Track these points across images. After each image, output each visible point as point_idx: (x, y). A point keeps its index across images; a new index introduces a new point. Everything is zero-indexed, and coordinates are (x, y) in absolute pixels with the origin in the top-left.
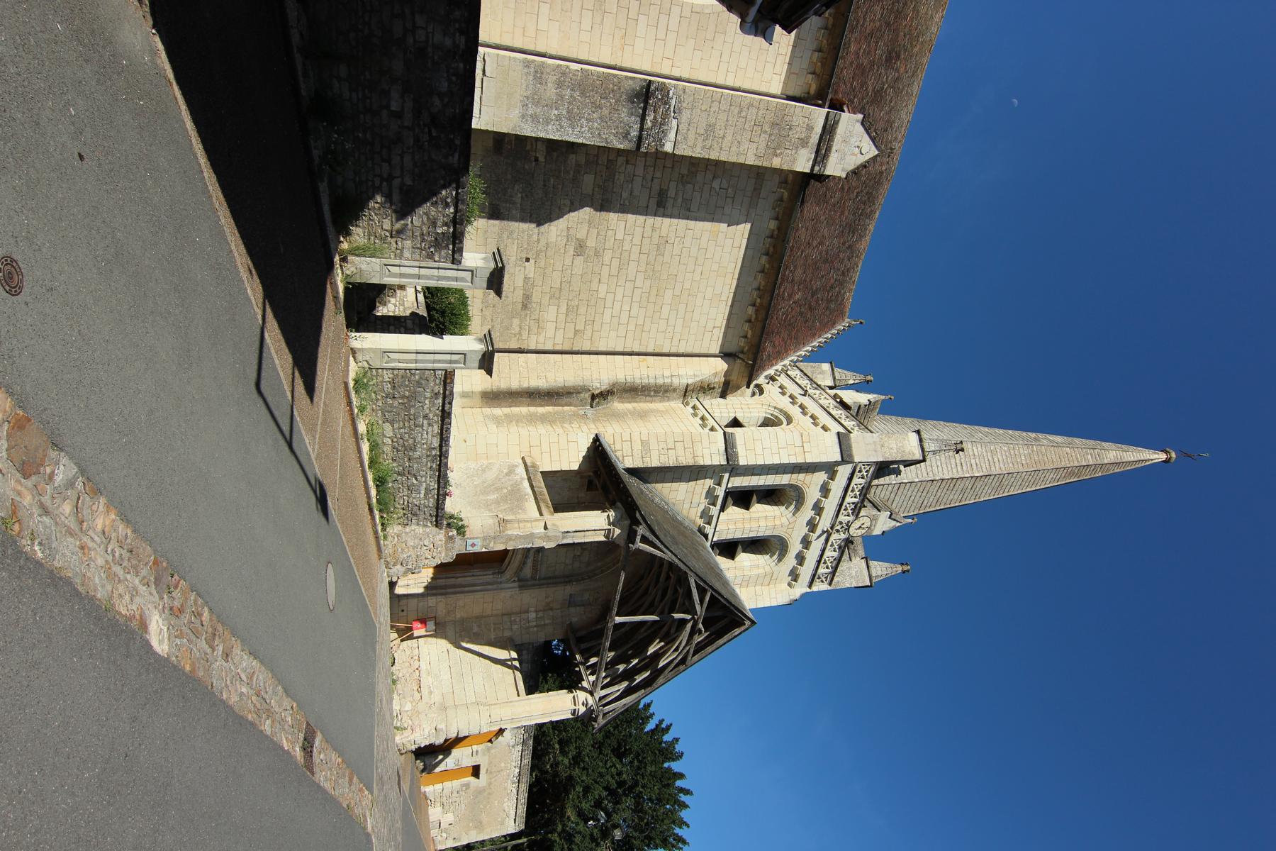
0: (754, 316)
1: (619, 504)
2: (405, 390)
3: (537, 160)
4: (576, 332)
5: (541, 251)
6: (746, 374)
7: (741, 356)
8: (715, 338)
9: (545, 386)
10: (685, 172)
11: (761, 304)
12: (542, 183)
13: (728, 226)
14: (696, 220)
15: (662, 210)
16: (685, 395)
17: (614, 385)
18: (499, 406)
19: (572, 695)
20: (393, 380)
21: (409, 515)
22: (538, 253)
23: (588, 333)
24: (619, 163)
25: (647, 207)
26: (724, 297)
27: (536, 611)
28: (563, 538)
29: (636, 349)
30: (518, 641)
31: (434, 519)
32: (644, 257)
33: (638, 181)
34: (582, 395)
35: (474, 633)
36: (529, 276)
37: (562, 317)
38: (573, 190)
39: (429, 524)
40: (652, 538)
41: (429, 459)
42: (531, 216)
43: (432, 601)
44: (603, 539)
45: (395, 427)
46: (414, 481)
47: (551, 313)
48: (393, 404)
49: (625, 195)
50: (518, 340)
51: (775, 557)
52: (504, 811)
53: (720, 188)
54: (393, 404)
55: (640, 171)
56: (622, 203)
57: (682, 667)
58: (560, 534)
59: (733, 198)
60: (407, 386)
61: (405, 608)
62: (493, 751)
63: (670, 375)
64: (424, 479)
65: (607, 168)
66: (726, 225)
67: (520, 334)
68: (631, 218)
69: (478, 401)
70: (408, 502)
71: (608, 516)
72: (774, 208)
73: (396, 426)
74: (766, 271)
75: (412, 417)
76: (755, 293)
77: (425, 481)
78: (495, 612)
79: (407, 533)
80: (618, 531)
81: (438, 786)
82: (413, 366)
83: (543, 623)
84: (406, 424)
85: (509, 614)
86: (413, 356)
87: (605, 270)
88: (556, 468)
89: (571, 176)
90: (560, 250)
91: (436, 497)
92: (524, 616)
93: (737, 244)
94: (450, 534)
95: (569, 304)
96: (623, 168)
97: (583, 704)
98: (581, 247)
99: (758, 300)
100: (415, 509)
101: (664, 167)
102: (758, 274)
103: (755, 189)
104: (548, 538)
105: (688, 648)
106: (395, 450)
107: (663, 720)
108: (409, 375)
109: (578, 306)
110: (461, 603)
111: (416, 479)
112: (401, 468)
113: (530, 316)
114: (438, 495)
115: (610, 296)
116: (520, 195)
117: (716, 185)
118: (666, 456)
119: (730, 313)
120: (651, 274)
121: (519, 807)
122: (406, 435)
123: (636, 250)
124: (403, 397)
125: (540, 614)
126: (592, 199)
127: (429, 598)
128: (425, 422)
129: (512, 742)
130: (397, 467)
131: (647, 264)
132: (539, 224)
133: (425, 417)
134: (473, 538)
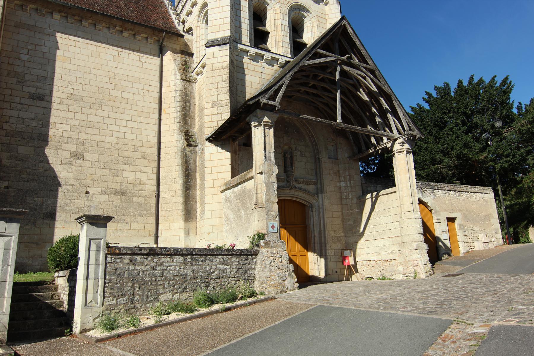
0: (130, 32)
1: (247, 119)
2: (126, 286)
3: (7, 187)
4: (143, 158)
5: (80, 183)
6: (175, 38)
7: (161, 41)
8: (148, 60)
9: (181, 179)
10: (15, 80)
11: (121, 26)
12: (26, 183)
13: (58, 49)
14: (53, 73)
15: (46, 98)
16: (190, 81)
17: (181, 131)
18: (195, 210)
19: (396, 154)
20: (115, 296)
21: (246, 276)
22: (81, 185)
23: (144, 149)
24: (9, 128)
25: (44, 108)
26: (116, 53)
27: (340, 182)
28: (270, 160)
29: (156, 116)
30: (360, 193)
31: (250, 257)
32: (84, 110)
33: (22, 114)
34: (188, 153)
35: (354, 223)
36: (100, 192)
37: (132, 168)
38: (31, 161)
39: (255, 260)
40: (271, 92)
41: (194, 263)
42: (52, 191)
43: (330, 252)
44: (272, 130)
45: (163, 292)
46: (215, 273)
47: (129, 176)
48: (139, 295)
49: (34, 124)
50: (149, 198)
51: (305, 14)
52: (479, 201)
53: (28, 54)
54: (139, 295)
55: (14, 113)
56: (41, 126)
57: (377, 73)
58: (266, 162)
59: (35, 45)
60: (122, 285)
61: (335, 271)
62: (438, 209)
63: (174, 92)
64: (213, 267)
65: (13, 137)
66: (58, 51)
67: (145, 197)
68: (53, 119)
69: (191, 225)
70: (234, 277)
71: (255, 126)
72: (44, 15)
73: (161, 291)
74: (94, 22)
75: (153, 279)
76: (112, 30)
77: (216, 265)
78: (340, 210)
79: (260, 278)
80: (266, 119)
81: (460, 244)
82: (101, 282)
84: (160, 283)
85: (341, 200)
86: (91, 282)
87: (94, 138)
88: (229, 168)
89: (19, 162)
90: (79, 170)
91: (230, 257)
92: (343, 189)
93: (73, 43)
94: (263, 244)
95: (121, 163)
96: (12, 125)
97: (403, 146)
98: (77, 155)
99: (118, 28)
100: (241, 272)
101: (11, 95)
102: (97, 28)
103: (28, 29)
104: (269, 173)
105: (362, 68)
106: (185, 290)
107: (423, 98)
108: (110, 284)
109: (124, 157)
110: (332, 233)
111: (213, 272)
112: (203, 285)
113: (131, 190)
114: (228, 255)
115: (116, 134)
116: (36, 199)
117: (25, 58)
118: (222, 89)
119: (128, 49)
120: (98, 105)
121: (476, 191)
122: (171, 282)
123: (78, 116)
124: (133, 287)
125: (342, 179)
126: (38, 147)
127: (328, 254)
128: (158, 268)
129: (432, 196)
130: (201, 288)
131: (90, 108)
132: (59, 185)
133: (154, 268)
134: (267, 227)
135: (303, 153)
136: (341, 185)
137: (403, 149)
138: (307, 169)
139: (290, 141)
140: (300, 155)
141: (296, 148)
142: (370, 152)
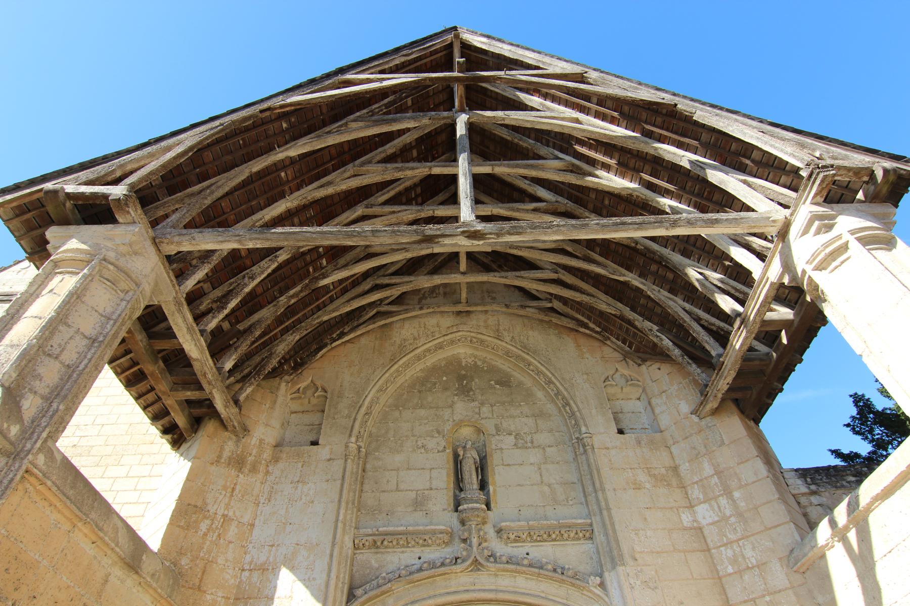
19: (822, 279)
27: (691, 507)
30: (788, 533)
83: (715, 479)
85: (719, 580)
97: (830, 227)
125: (696, 493)
135: (529, 439)
136: (700, 519)
137: (839, 237)
138: (549, 486)
139: (477, 410)
140: (515, 445)
141: (498, 429)
142: (737, 347)
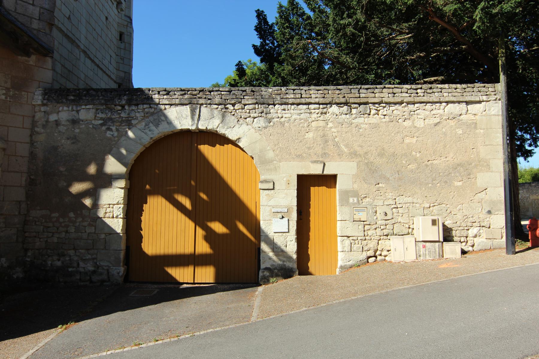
52: (436, 125)
62: (270, 154)
81: (341, 245)
121: (435, 97)
129: (260, 122)
